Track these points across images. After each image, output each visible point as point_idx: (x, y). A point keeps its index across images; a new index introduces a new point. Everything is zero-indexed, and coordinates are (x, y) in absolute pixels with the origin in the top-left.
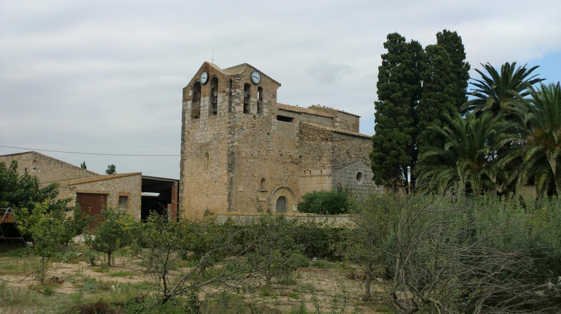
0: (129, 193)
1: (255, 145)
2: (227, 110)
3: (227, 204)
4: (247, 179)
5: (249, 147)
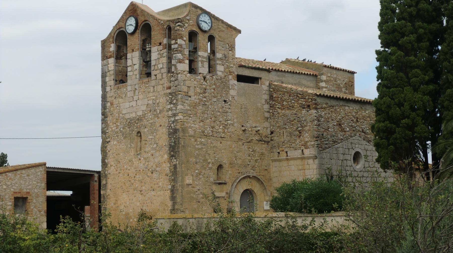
0: (28, 193)
1: (207, 118)
2: (165, 70)
3: (170, 204)
4: (198, 166)
5: (198, 120)
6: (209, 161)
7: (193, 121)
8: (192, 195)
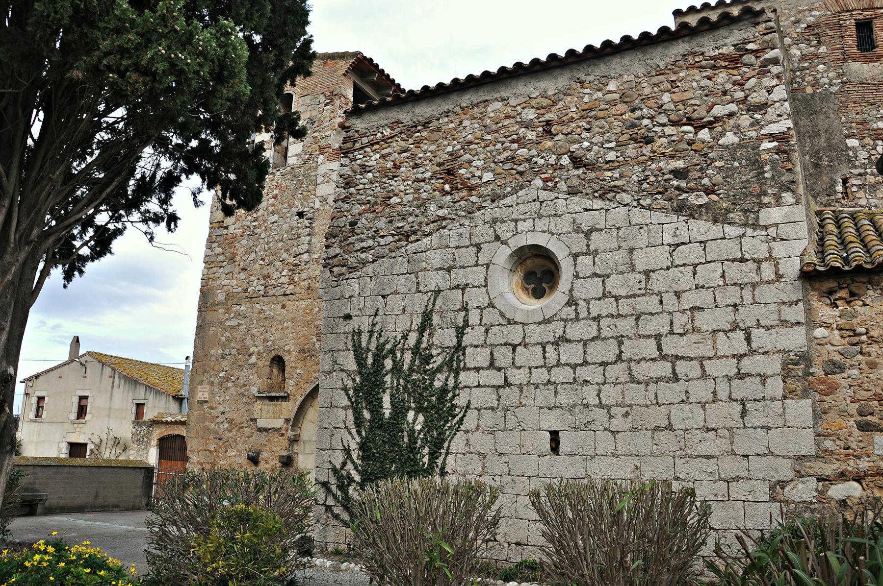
1: (255, 261)
4: (225, 364)
5: (237, 270)
6: (251, 350)
7: (227, 274)
8: (207, 423)
